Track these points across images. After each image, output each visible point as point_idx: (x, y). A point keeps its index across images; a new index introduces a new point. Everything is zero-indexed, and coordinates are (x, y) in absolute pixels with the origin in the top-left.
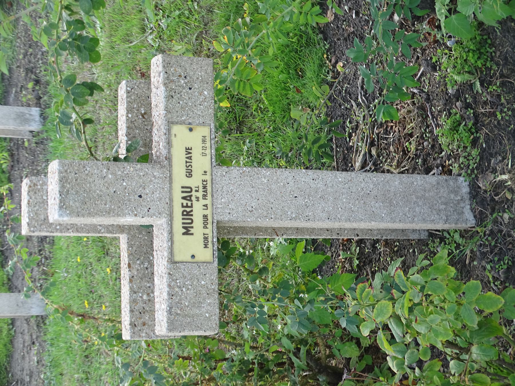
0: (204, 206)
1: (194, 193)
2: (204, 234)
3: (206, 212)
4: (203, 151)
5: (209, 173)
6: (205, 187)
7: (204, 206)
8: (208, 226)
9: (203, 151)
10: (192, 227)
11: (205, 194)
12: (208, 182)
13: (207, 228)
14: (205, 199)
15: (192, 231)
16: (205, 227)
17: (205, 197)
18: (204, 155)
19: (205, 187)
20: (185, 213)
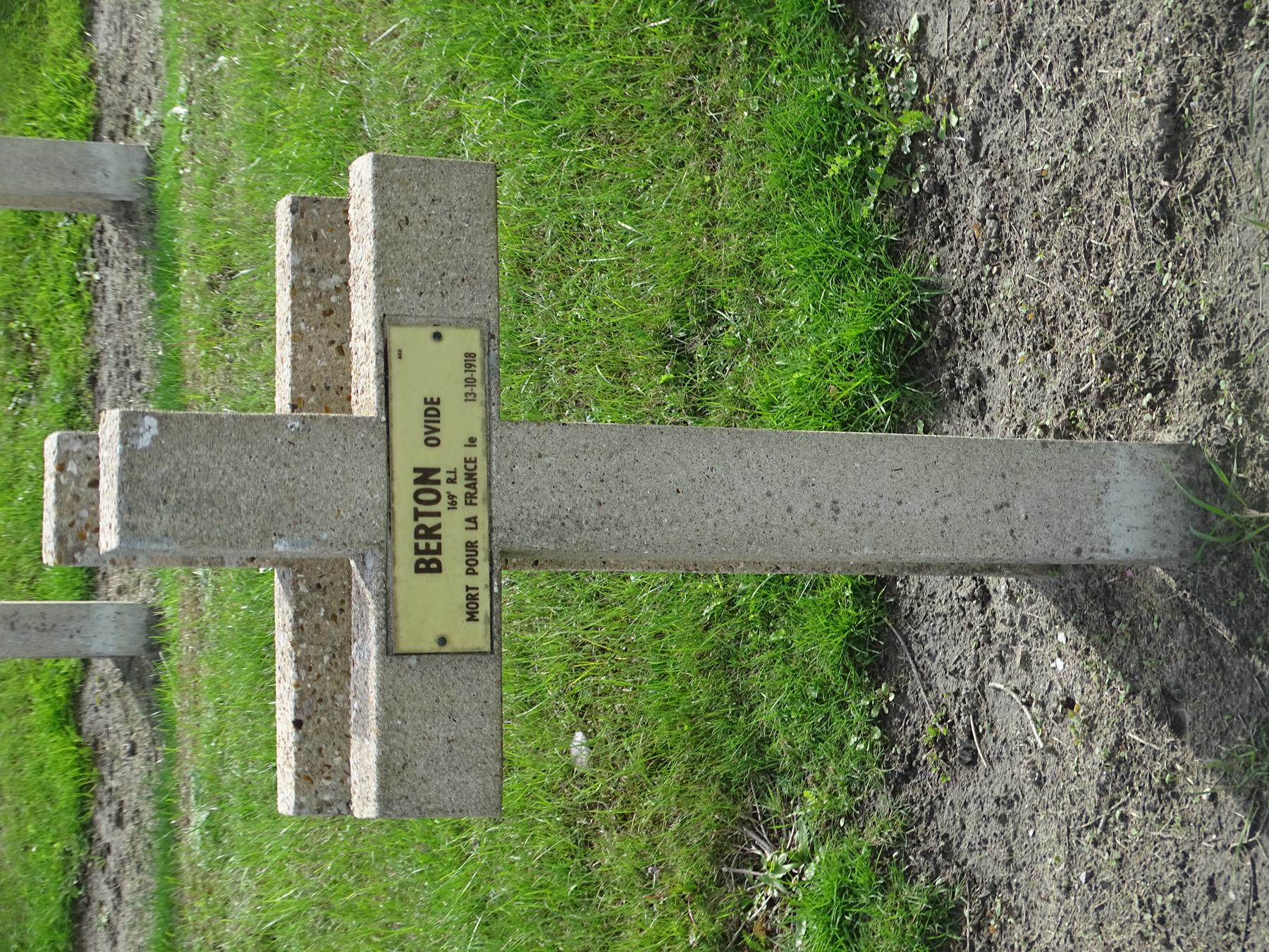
0: (468, 520)
1: (443, 488)
2: (468, 588)
4: (468, 389)
5: (480, 442)
6: (471, 475)
7: (468, 520)
8: (476, 569)
9: (468, 389)
11: (472, 491)
12: (479, 464)
13: (475, 573)
14: (471, 504)
16: (471, 571)
17: (470, 499)
18: (470, 397)
19: (471, 475)
20: (422, 532)
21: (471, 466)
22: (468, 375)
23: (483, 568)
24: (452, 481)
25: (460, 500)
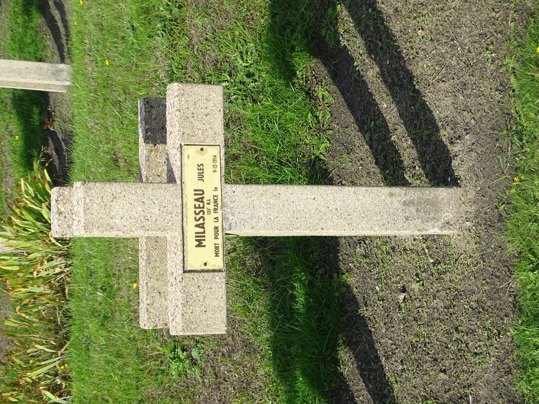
0: (215, 218)
1: (206, 206)
2: (215, 244)
3: (216, 224)
4: (214, 169)
5: (219, 189)
6: (216, 201)
7: (215, 218)
10: (204, 240)
12: (219, 197)
13: (218, 238)
15: (204, 243)
16: (216, 238)
17: (215, 210)
18: (215, 171)
19: (216, 201)
21: (216, 198)
22: (214, 164)
23: (220, 236)
24: (209, 204)
25: (212, 211)
